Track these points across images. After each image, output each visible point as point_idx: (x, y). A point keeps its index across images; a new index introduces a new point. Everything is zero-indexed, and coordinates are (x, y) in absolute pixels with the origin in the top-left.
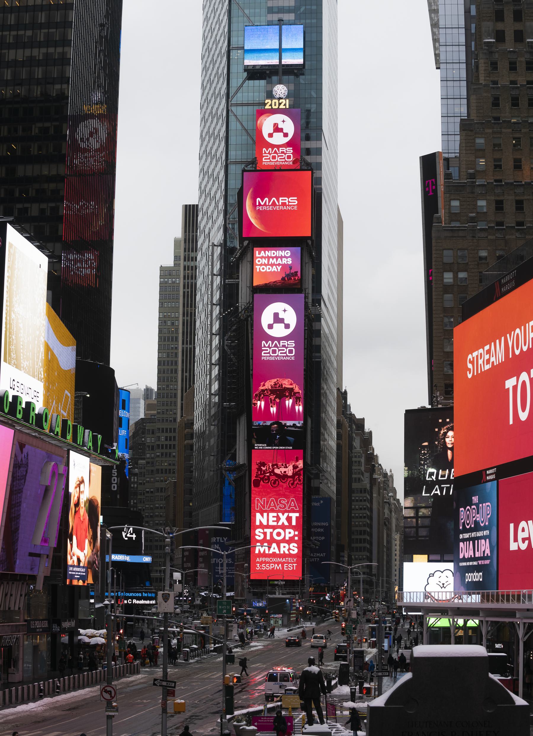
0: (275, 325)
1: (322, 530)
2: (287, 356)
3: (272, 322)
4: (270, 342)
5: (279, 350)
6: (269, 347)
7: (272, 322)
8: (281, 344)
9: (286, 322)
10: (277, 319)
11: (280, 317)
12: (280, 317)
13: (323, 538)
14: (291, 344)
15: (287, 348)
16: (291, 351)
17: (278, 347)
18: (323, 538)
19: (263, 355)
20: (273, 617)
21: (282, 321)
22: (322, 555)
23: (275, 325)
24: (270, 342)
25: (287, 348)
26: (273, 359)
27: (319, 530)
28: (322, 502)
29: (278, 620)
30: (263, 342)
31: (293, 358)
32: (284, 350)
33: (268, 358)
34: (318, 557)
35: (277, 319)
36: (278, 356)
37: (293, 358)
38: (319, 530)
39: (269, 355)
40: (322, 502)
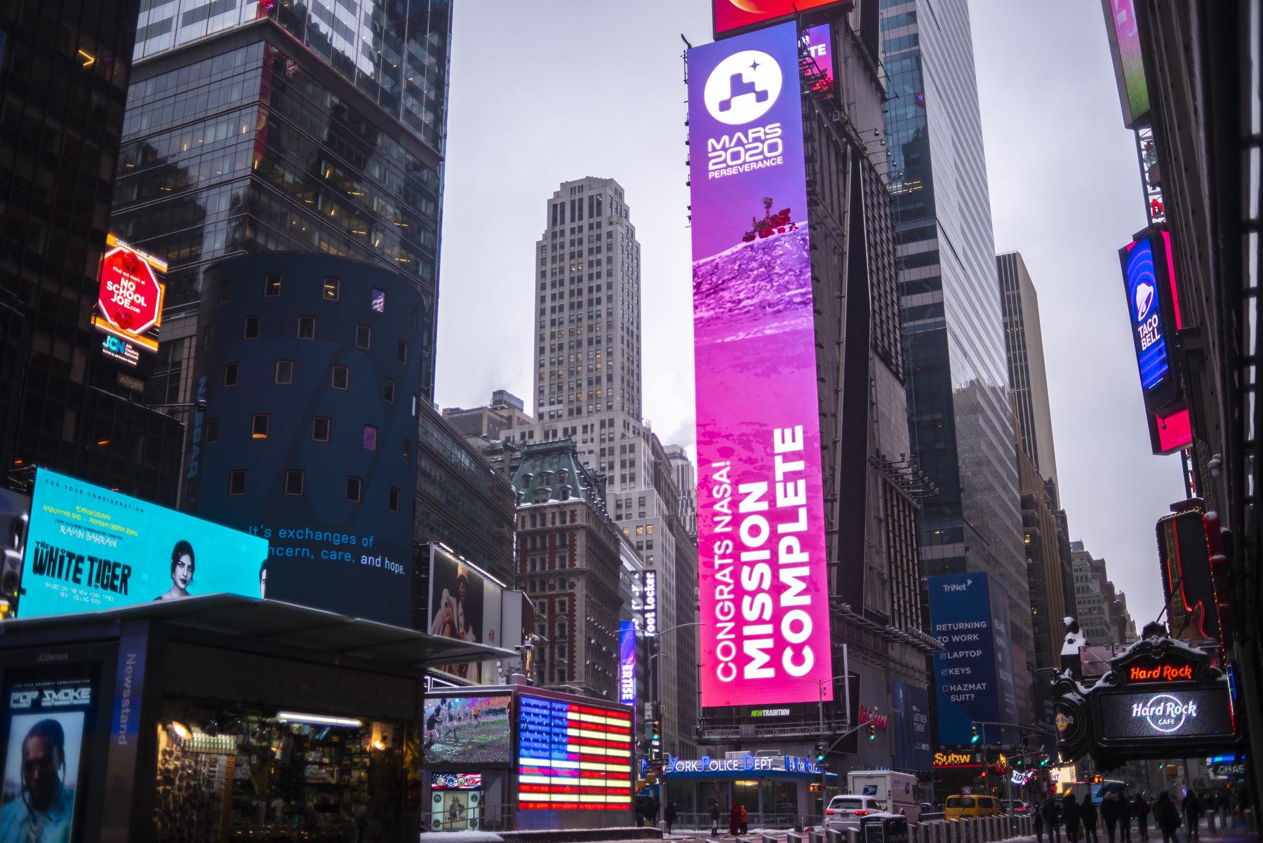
0: (735, 101)
1: (975, 637)
2: (766, 158)
3: (727, 95)
4: (726, 138)
5: (747, 151)
6: (724, 149)
7: (727, 95)
8: (751, 136)
9: (758, 88)
10: (739, 86)
11: (746, 80)
12: (746, 80)
13: (979, 653)
14: (774, 130)
15: (763, 142)
16: (773, 147)
17: (743, 145)
18: (979, 653)
19: (711, 167)
20: (444, 788)
21: (750, 88)
22: (979, 687)
23: (735, 101)
24: (726, 138)
25: (763, 142)
26: (734, 171)
27: (969, 637)
28: (970, 582)
29: (462, 798)
30: (711, 141)
31: (779, 161)
32: (757, 148)
33: (724, 173)
34: (972, 691)
35: (739, 86)
36: (745, 163)
37: (779, 161)
38: (969, 637)
39: (724, 165)
40: (970, 582)
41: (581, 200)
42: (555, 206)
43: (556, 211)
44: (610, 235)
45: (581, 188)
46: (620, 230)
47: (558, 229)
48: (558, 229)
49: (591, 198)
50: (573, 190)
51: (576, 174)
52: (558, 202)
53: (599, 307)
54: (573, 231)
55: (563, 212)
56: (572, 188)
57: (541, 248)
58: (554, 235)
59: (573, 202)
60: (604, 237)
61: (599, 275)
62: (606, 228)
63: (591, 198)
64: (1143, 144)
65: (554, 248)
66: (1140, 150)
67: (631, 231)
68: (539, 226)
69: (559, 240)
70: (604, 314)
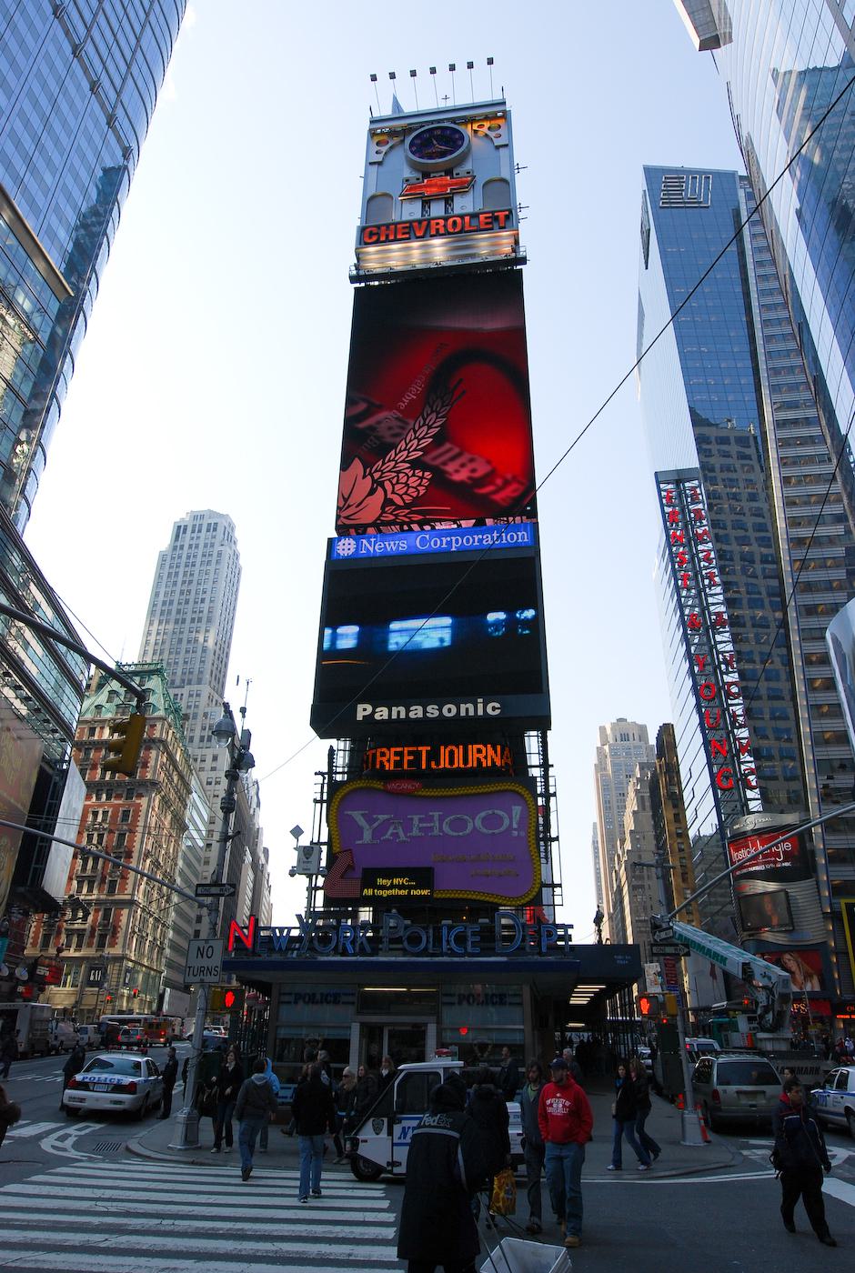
41: (201, 525)
42: (179, 527)
43: (180, 530)
44: (220, 554)
45: (202, 517)
46: (227, 551)
47: (178, 544)
48: (178, 544)
49: (209, 525)
50: (195, 517)
51: (200, 506)
52: (182, 524)
53: (202, 605)
54: (190, 546)
55: (185, 532)
56: (198, 517)
57: (163, 558)
58: (175, 548)
59: (194, 526)
60: (215, 554)
61: (209, 563)
62: (217, 548)
63: (209, 525)
64: (664, 494)
65: (173, 558)
66: (661, 498)
67: (236, 556)
68: (164, 541)
69: (178, 552)
70: (206, 611)
